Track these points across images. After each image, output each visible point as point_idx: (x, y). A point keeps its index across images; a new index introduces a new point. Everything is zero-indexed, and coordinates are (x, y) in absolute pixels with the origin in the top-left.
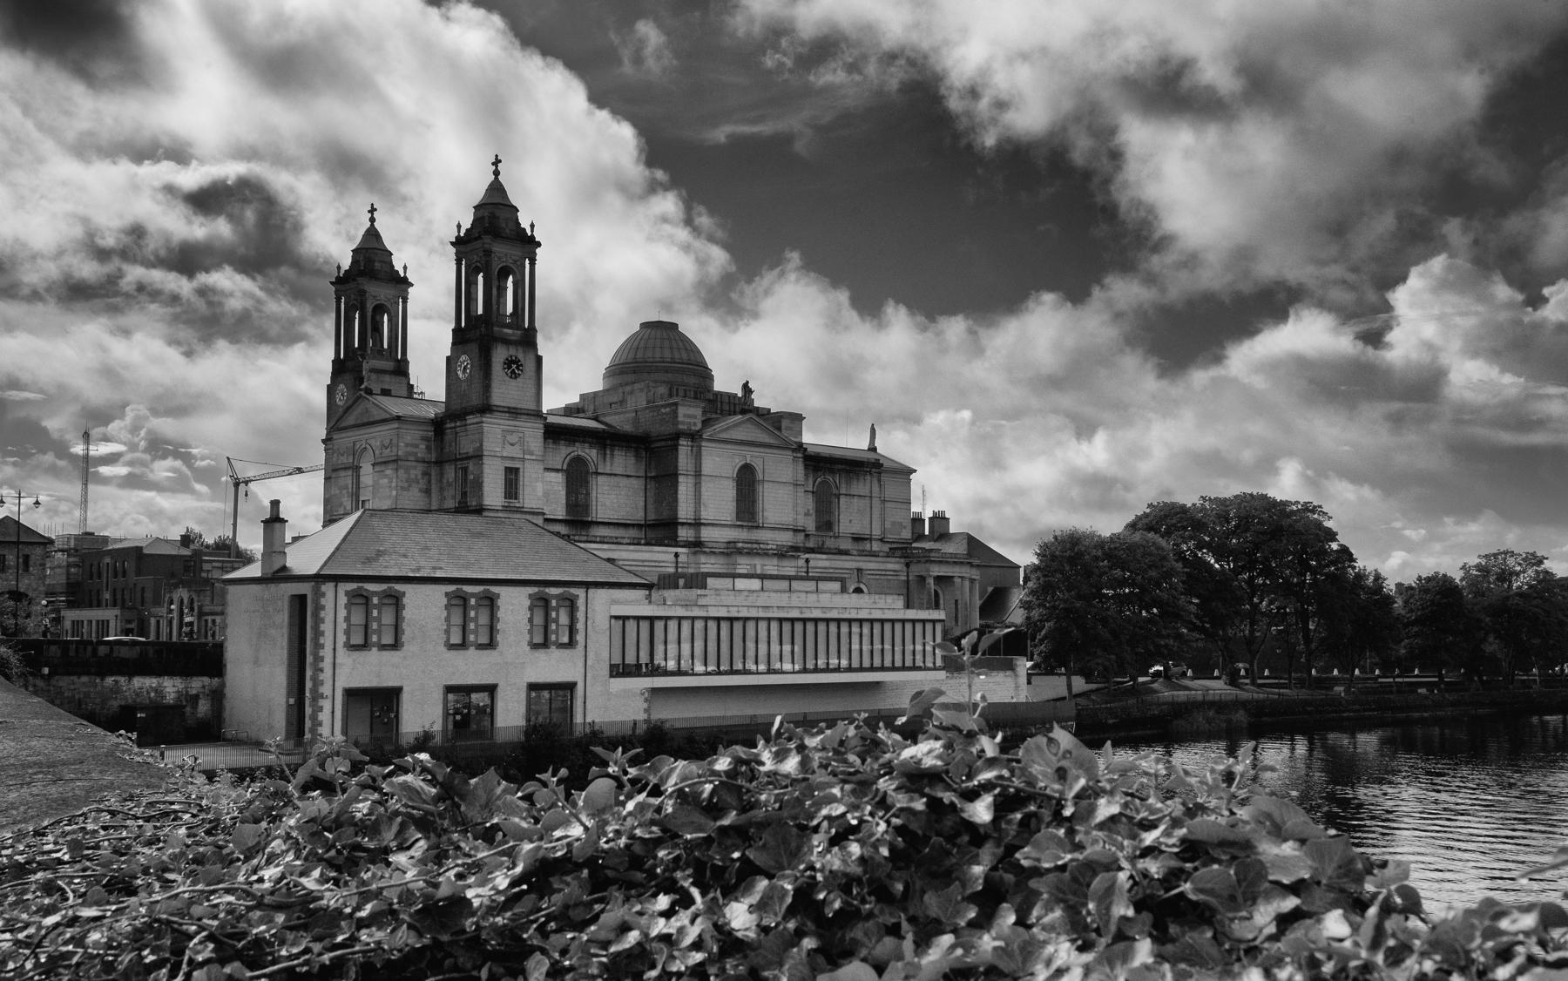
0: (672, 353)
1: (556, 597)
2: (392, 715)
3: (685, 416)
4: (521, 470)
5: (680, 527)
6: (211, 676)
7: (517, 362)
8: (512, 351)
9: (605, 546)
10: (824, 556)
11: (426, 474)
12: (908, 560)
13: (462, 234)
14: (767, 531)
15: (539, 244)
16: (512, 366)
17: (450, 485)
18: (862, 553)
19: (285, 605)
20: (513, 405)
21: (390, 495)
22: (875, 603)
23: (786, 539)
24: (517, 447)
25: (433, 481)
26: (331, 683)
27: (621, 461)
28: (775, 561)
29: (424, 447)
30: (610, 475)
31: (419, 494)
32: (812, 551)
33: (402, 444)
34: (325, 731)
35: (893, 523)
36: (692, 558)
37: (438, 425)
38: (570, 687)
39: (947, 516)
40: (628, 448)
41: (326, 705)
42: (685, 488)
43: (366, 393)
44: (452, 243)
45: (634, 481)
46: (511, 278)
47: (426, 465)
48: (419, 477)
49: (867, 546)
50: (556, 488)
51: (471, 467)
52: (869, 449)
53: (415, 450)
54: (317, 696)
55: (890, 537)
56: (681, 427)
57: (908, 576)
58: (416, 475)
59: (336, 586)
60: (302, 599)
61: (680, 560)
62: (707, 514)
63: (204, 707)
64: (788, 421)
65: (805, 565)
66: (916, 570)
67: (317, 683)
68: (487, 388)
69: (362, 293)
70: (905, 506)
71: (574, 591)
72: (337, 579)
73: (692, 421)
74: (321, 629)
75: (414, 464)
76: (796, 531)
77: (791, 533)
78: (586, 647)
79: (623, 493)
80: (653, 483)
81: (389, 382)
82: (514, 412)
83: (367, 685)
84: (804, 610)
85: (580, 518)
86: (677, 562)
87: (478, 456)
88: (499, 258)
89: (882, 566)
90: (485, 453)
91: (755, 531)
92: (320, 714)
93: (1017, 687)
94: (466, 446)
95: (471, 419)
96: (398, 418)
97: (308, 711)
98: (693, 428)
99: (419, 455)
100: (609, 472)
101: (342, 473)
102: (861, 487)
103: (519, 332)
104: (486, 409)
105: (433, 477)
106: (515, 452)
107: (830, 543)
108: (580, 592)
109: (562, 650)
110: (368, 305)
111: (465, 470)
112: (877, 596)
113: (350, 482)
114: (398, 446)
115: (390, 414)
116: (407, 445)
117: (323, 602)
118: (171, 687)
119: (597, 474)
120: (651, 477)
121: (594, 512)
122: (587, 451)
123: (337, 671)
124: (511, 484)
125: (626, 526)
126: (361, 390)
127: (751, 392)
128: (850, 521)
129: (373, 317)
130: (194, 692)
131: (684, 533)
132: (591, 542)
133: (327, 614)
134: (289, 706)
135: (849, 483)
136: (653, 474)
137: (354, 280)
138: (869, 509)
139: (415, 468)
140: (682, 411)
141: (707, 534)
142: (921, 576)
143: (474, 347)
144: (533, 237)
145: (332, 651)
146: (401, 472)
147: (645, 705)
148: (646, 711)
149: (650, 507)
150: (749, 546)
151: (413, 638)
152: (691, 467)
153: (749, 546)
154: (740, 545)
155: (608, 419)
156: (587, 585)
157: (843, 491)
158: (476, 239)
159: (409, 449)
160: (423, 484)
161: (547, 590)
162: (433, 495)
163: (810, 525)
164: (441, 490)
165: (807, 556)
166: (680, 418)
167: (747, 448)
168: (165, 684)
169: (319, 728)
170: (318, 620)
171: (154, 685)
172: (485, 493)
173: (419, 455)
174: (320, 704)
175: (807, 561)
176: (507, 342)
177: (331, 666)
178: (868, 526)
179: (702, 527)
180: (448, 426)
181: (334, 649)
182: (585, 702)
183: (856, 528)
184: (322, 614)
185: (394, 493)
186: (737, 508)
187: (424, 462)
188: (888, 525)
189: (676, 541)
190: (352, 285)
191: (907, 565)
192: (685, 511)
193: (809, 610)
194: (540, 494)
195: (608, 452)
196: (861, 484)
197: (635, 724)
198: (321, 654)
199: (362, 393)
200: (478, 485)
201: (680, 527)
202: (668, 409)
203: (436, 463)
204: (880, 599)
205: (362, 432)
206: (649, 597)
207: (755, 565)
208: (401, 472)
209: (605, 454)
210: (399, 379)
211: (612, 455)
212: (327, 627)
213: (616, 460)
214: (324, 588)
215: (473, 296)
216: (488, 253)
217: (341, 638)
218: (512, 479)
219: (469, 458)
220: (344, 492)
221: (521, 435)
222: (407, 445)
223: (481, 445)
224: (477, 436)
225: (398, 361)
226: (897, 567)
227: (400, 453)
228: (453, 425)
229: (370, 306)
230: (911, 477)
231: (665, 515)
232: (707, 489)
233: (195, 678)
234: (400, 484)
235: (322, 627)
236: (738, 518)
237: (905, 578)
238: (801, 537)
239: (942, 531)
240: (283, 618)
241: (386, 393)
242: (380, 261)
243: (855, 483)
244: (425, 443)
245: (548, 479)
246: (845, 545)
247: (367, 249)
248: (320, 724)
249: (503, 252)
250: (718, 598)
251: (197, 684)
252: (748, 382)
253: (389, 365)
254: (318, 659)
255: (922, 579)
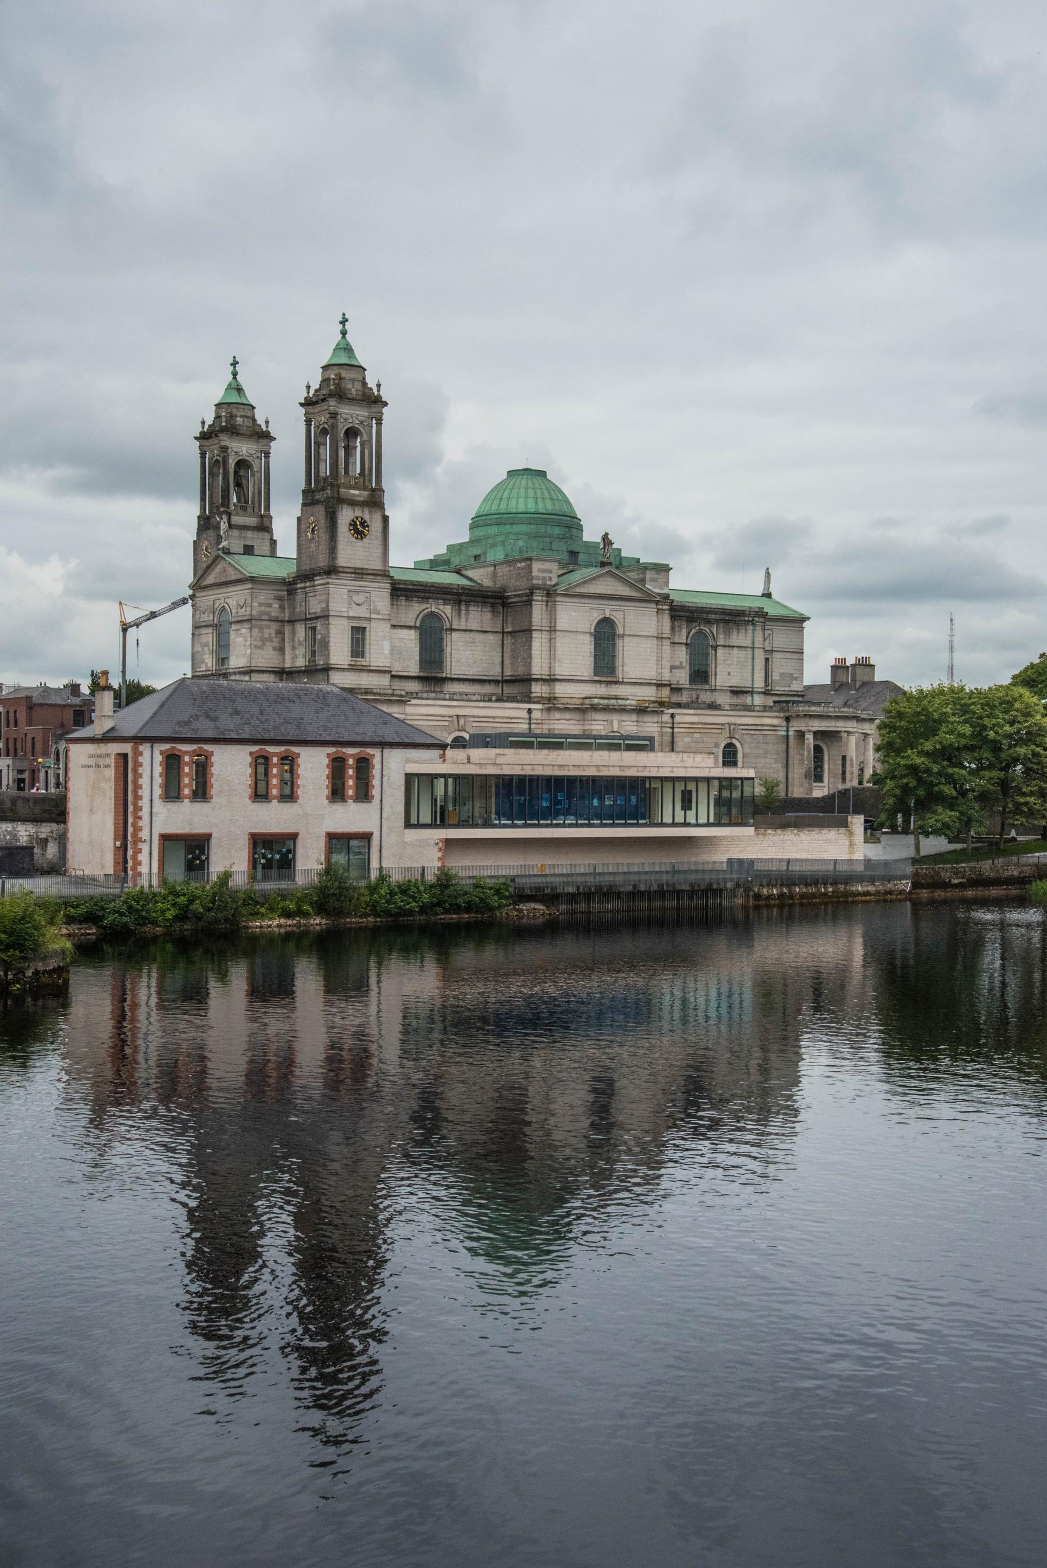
0: (537, 504)
1: (352, 756)
2: (203, 858)
3: (539, 570)
4: (368, 629)
5: (533, 683)
6: (58, 823)
7: (363, 523)
8: (358, 512)
9: (455, 703)
10: (692, 711)
11: (280, 633)
12: (787, 714)
13: (311, 395)
14: (626, 686)
15: (385, 404)
16: (359, 530)
17: (300, 644)
18: (734, 707)
19: (111, 761)
20: (359, 566)
21: (245, 654)
22: (683, 761)
23: (649, 694)
24: (364, 607)
25: (287, 640)
26: (149, 829)
27: (477, 617)
28: (634, 717)
29: (276, 606)
30: (465, 630)
31: (272, 652)
32: (679, 705)
33: (255, 604)
34: (144, 869)
35: (782, 675)
36: (545, 715)
37: (289, 588)
38: (367, 837)
39: (872, 663)
40: (484, 603)
41: (145, 847)
42: (539, 643)
43: (224, 553)
44: (301, 404)
45: (491, 637)
46: (359, 439)
47: (280, 624)
48: (273, 635)
49: (748, 700)
50: (409, 645)
51: (319, 628)
52: (763, 595)
53: (268, 609)
54: (137, 840)
55: (779, 688)
56: (535, 582)
57: (788, 731)
58: (270, 634)
59: (152, 747)
60: (125, 756)
61: (533, 715)
62: (562, 670)
63: (52, 850)
64: (653, 572)
65: (670, 720)
66: (796, 725)
67: (137, 829)
68: (333, 550)
69: (224, 449)
70: (797, 656)
71: (370, 751)
72: (153, 740)
73: (548, 575)
74: (140, 783)
75: (268, 623)
76: (659, 685)
77: (654, 688)
78: (381, 801)
79: (478, 648)
80: (509, 638)
81: (252, 538)
82: (360, 573)
83: (179, 831)
84: (601, 768)
85: (433, 675)
86: (530, 719)
87: (325, 617)
88: (346, 420)
89: (758, 721)
90: (331, 613)
91: (614, 686)
92: (139, 855)
93: (852, 844)
94: (315, 607)
95: (319, 581)
96: (252, 579)
97: (130, 852)
98: (548, 583)
99: (273, 614)
100: (464, 628)
101: (204, 631)
102: (740, 638)
103: (366, 493)
104: (332, 570)
105: (287, 636)
106: (362, 612)
107: (706, 697)
108: (376, 752)
109: (358, 804)
110: (230, 461)
111: (314, 629)
112: (685, 755)
113: (211, 639)
114: (251, 606)
115: (244, 575)
116: (260, 605)
117: (141, 759)
118: (24, 833)
119: (452, 630)
120: (508, 633)
121: (448, 668)
122: (441, 607)
123: (154, 819)
124: (357, 645)
125: (482, 682)
126: (219, 549)
127: (611, 544)
128: (729, 674)
129: (236, 473)
130: (43, 836)
131: (537, 689)
132: (440, 699)
133: (145, 771)
134: (116, 848)
135: (727, 634)
136: (509, 630)
137: (216, 435)
138: (750, 660)
139: (269, 627)
140: (536, 566)
141: (560, 690)
142: (800, 731)
143: (320, 510)
144: (380, 396)
145: (149, 802)
146: (255, 631)
147: (440, 854)
148: (440, 859)
149: (507, 662)
150: (606, 702)
151: (221, 792)
152: (545, 623)
153: (606, 702)
154: (596, 701)
155: (470, 573)
156: (383, 745)
157: (721, 642)
158: (323, 400)
159: (263, 608)
160: (276, 643)
161: (344, 750)
162: (287, 653)
163: (682, 677)
164: (293, 648)
165: (671, 711)
166: (535, 573)
167: (606, 602)
168: (19, 829)
169: (139, 867)
170: (137, 776)
171: (9, 829)
172: (332, 653)
173: (273, 614)
174: (139, 847)
175: (673, 716)
176: (353, 503)
177: (149, 814)
178: (750, 678)
179: (557, 683)
180: (299, 586)
181: (151, 800)
182: (380, 851)
183: (735, 681)
184: (140, 770)
185: (249, 651)
186: (595, 663)
187: (278, 621)
188: (776, 676)
189: (529, 697)
190: (214, 441)
191: (788, 719)
192: (538, 668)
193: (606, 769)
194: (387, 652)
195: (463, 608)
196: (742, 635)
197: (423, 870)
198: (140, 804)
199: (220, 552)
200: (325, 644)
201: (533, 683)
202: (523, 564)
203: (289, 621)
204: (688, 757)
205: (221, 591)
206: (443, 757)
207: (612, 721)
208: (255, 631)
209: (460, 610)
210: (261, 534)
211: (467, 611)
212: (144, 781)
213: (471, 616)
214: (141, 748)
215: (322, 457)
216: (334, 415)
217: (158, 791)
218: (358, 636)
219: (317, 618)
220: (206, 649)
221: (367, 595)
222: (260, 605)
223: (328, 606)
224: (324, 597)
225: (262, 516)
226: (775, 722)
227: (254, 613)
228: (303, 585)
229: (232, 462)
230: (805, 625)
231: (520, 671)
232: (562, 642)
233: (44, 824)
234: (255, 643)
235: (141, 781)
236: (596, 674)
237: (784, 733)
238: (666, 692)
239: (866, 679)
240: (110, 773)
241: (249, 550)
242: (242, 416)
243: (735, 633)
244: (278, 601)
245: (401, 636)
246: (723, 699)
247: (229, 404)
248: (140, 864)
249: (351, 414)
250: (517, 756)
251: (45, 830)
252: (607, 534)
253: (252, 521)
254: (138, 809)
255: (801, 735)
